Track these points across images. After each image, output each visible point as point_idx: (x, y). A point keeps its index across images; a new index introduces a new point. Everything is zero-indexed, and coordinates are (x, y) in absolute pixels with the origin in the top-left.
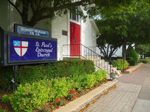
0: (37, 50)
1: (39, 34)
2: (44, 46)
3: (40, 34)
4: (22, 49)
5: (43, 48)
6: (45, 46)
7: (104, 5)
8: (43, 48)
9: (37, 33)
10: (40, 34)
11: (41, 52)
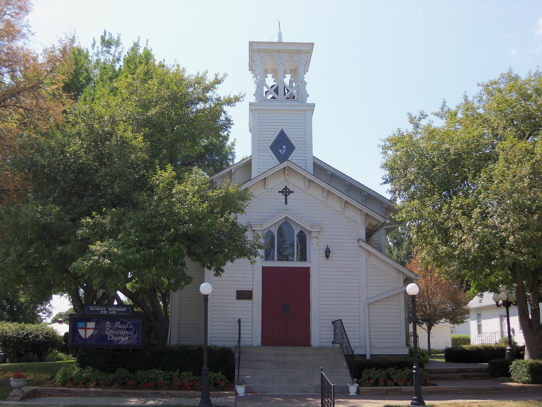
0: (107, 332)
1: (114, 312)
2: (119, 327)
3: (116, 311)
4: (88, 330)
5: (117, 329)
6: (120, 327)
7: (453, 114)
8: (117, 329)
9: (112, 311)
10: (116, 311)
11: (113, 334)
